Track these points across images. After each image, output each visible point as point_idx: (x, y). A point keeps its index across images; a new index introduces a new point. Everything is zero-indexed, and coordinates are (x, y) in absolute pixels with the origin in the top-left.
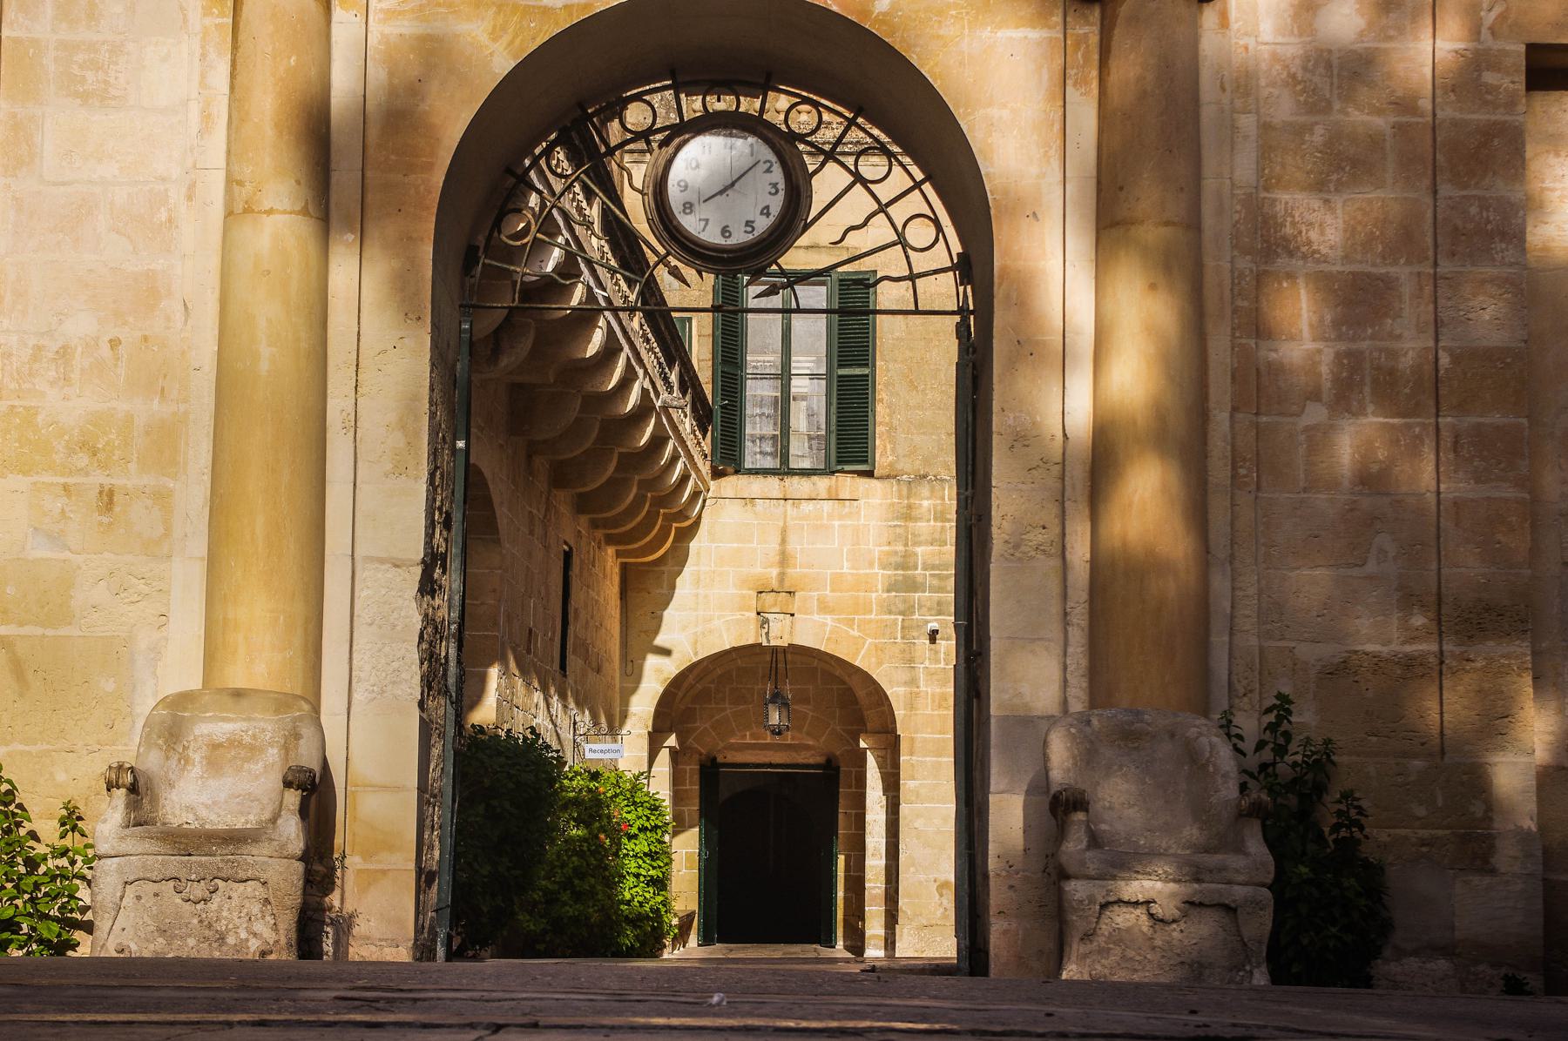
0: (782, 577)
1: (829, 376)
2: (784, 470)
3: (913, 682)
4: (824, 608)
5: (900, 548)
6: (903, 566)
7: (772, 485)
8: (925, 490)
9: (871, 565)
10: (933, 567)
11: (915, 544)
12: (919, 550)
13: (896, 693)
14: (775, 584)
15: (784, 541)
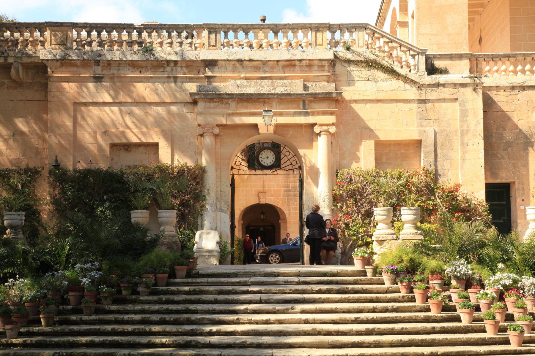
0: (263, 189)
3: (289, 210)
4: (272, 196)
9: (281, 187)
13: (286, 212)
15: (263, 183)
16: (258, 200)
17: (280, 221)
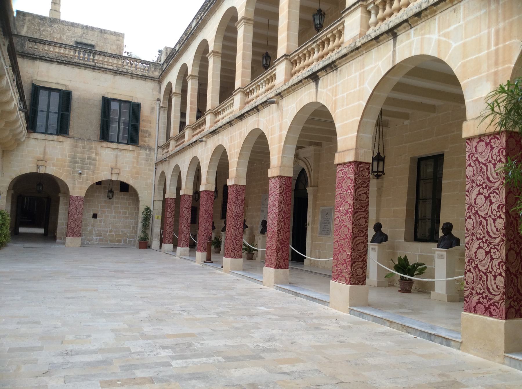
1: (58, 113)
2: (46, 133)
3: (74, 184)
4: (54, 165)
5: (73, 154)
6: (74, 158)
7: (43, 136)
8: (80, 142)
9: (66, 157)
11: (77, 153)
12: (78, 155)
13: (70, 186)
15: (45, 150)
17: (60, 195)
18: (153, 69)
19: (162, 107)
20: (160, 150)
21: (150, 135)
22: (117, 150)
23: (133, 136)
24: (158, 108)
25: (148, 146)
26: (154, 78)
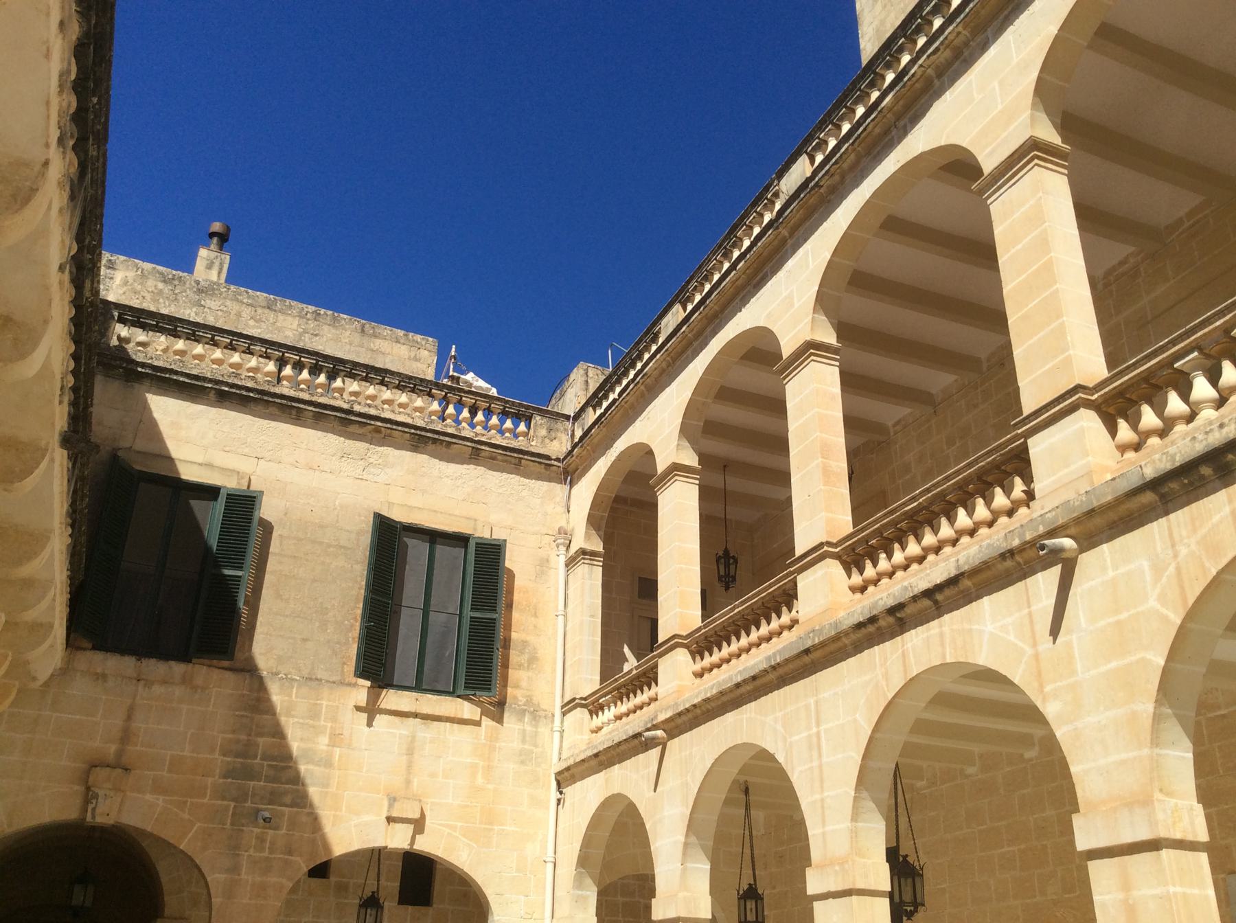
0: (120, 753)
3: (235, 869)
4: (158, 788)
5: (243, 737)
6: (243, 754)
10: (273, 758)
11: (261, 735)
12: (261, 741)
13: (216, 878)
14: (111, 758)
15: (129, 718)
16: (78, 801)
18: (543, 432)
19: (583, 552)
20: (581, 714)
21: (533, 659)
22: (412, 721)
23: (478, 665)
24: (562, 560)
25: (529, 701)
26: (548, 458)
